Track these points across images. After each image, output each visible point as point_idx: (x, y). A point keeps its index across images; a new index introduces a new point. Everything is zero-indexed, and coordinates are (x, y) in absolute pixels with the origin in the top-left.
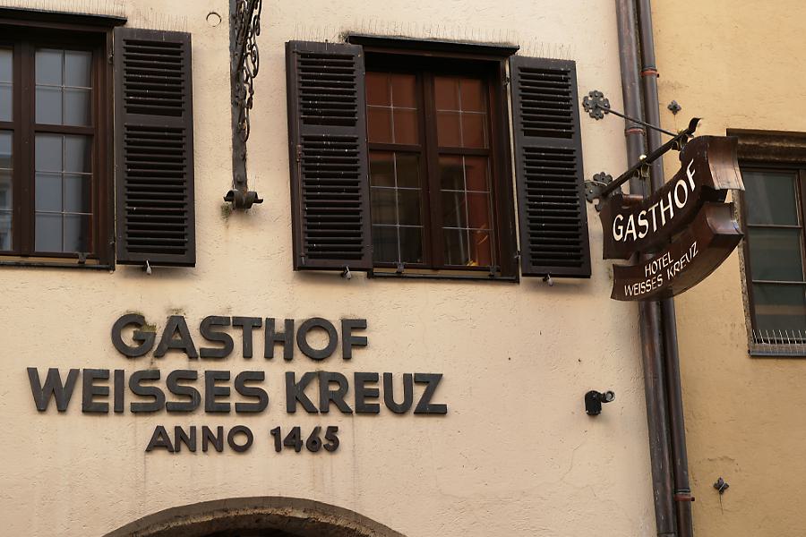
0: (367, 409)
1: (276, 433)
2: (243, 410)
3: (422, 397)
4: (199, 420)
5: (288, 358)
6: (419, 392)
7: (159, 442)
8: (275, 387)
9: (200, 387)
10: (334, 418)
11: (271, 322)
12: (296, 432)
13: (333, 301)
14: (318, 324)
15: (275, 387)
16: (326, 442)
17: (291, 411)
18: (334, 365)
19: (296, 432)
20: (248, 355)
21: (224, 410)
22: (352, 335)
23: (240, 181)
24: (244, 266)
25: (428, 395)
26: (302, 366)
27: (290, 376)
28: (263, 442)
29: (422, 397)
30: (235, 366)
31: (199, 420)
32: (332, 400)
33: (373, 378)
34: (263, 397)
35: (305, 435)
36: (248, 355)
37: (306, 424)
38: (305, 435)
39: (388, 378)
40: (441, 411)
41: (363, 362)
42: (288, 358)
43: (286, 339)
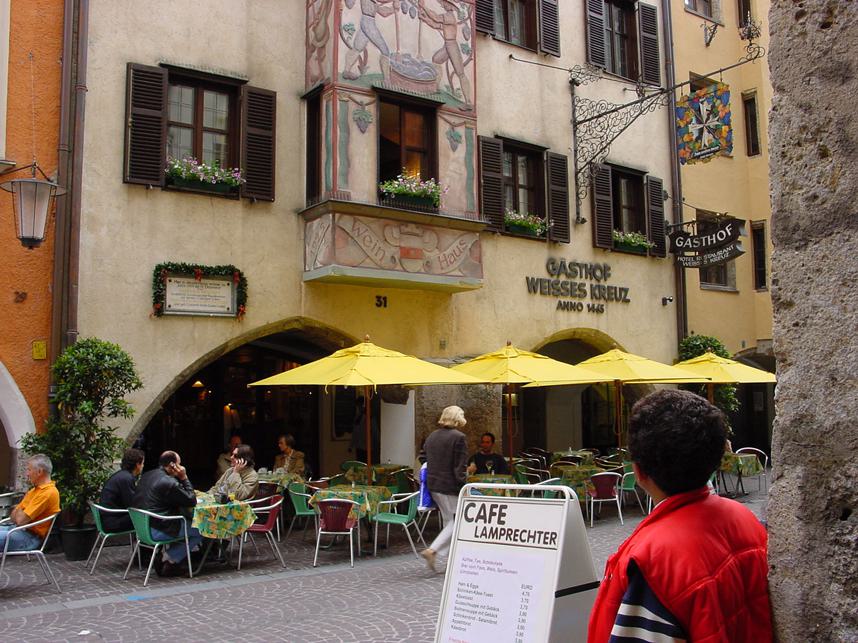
0: (609, 299)
1: (588, 306)
2: (579, 296)
3: (621, 296)
4: (568, 299)
5: (591, 279)
6: (623, 295)
7: (562, 307)
8: (587, 288)
9: (569, 286)
10: (602, 302)
11: (586, 265)
12: (593, 305)
13: (601, 260)
14: (598, 267)
15: (587, 288)
16: (600, 310)
17: (592, 298)
18: (602, 283)
19: (593, 305)
20: (581, 277)
21: (575, 296)
22: (606, 272)
23: (578, 213)
24: (579, 247)
25: (626, 295)
26: (594, 282)
27: (591, 285)
28: (585, 308)
29: (621, 296)
30: (578, 280)
31: (568, 299)
32: (602, 296)
33: (612, 288)
34: (585, 293)
35: (596, 306)
36: (581, 277)
37: (596, 303)
38: (596, 306)
39: (616, 288)
40: (628, 301)
41: (610, 283)
42: (591, 279)
43: (591, 271)
